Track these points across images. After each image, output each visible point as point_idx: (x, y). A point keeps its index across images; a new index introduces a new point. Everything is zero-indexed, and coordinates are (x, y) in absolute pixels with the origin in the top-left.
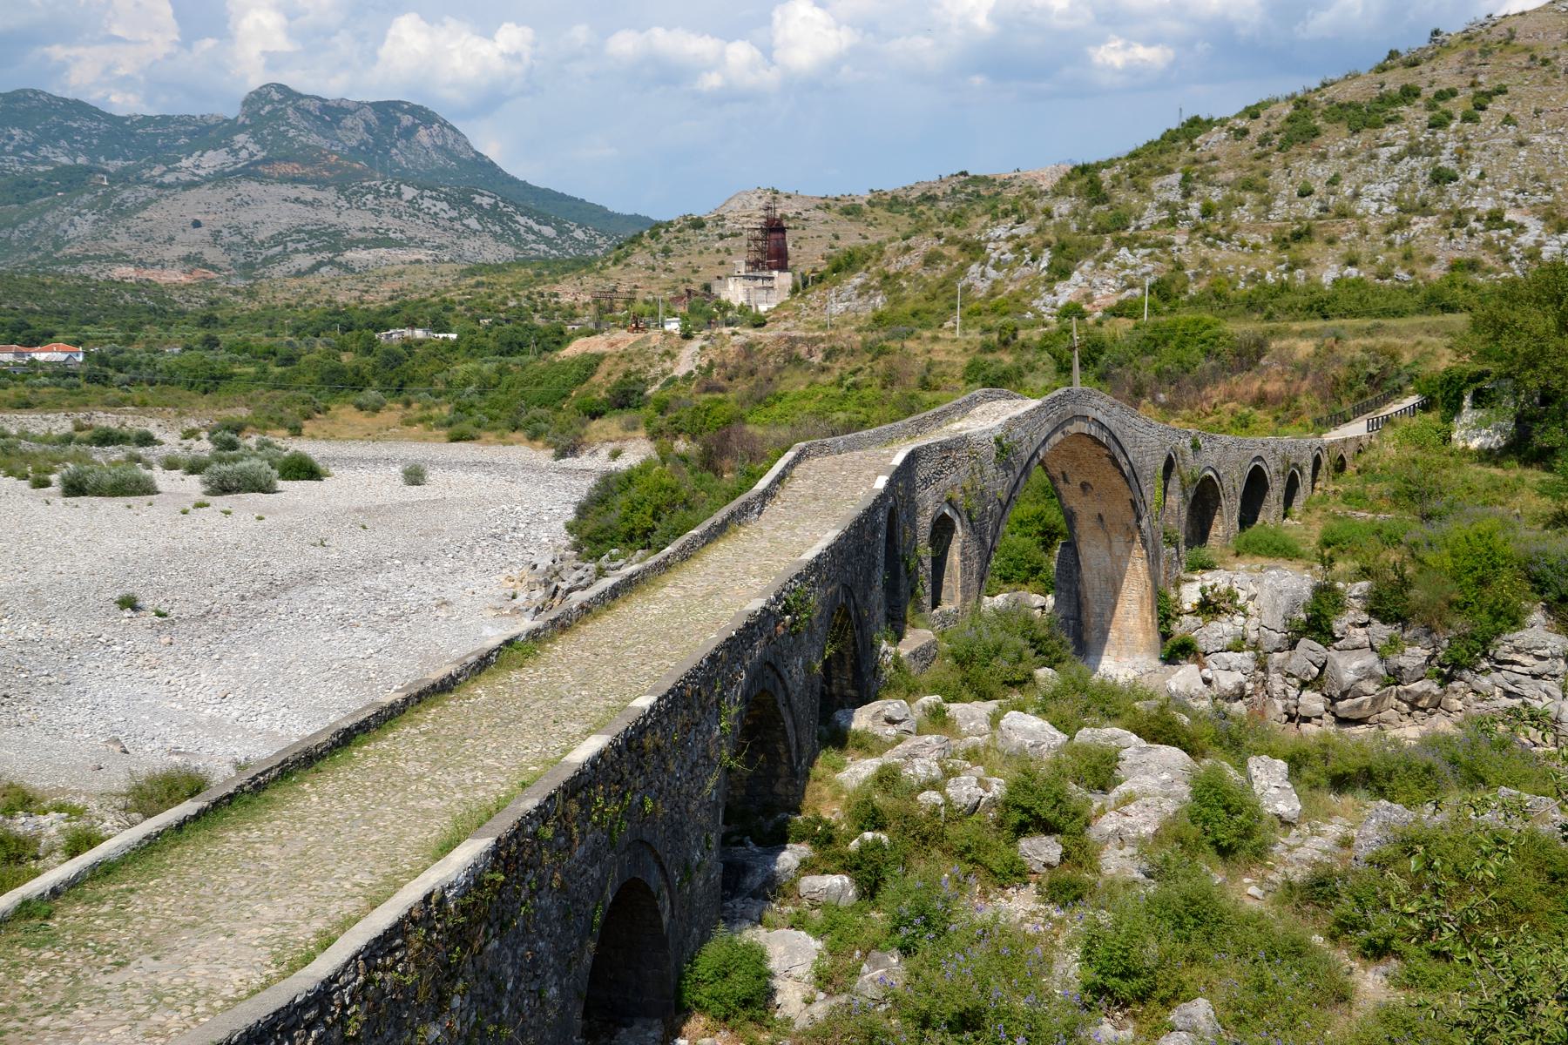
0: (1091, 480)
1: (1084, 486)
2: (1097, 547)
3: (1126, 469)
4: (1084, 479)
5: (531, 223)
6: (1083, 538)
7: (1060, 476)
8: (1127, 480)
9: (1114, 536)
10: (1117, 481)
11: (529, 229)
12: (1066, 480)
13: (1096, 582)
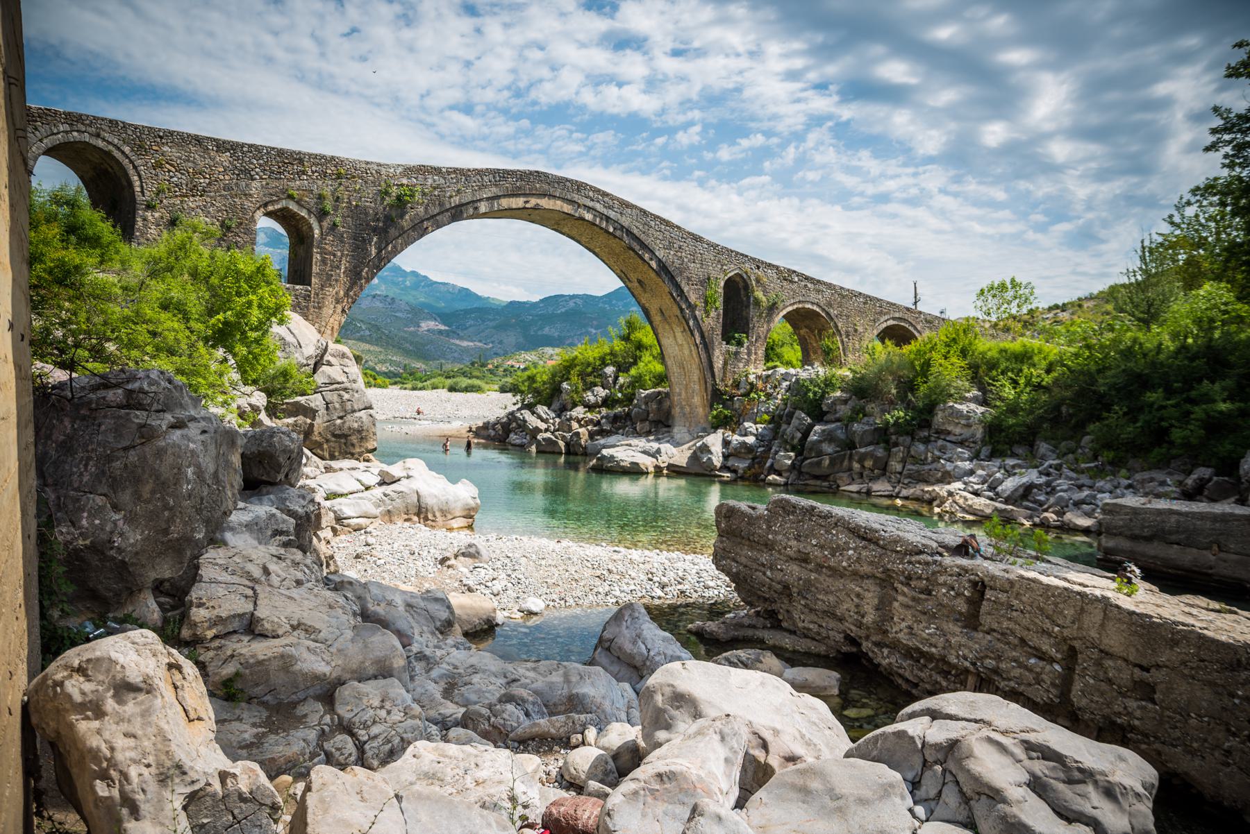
1: (640, 282)
9: (674, 326)
10: (653, 275)
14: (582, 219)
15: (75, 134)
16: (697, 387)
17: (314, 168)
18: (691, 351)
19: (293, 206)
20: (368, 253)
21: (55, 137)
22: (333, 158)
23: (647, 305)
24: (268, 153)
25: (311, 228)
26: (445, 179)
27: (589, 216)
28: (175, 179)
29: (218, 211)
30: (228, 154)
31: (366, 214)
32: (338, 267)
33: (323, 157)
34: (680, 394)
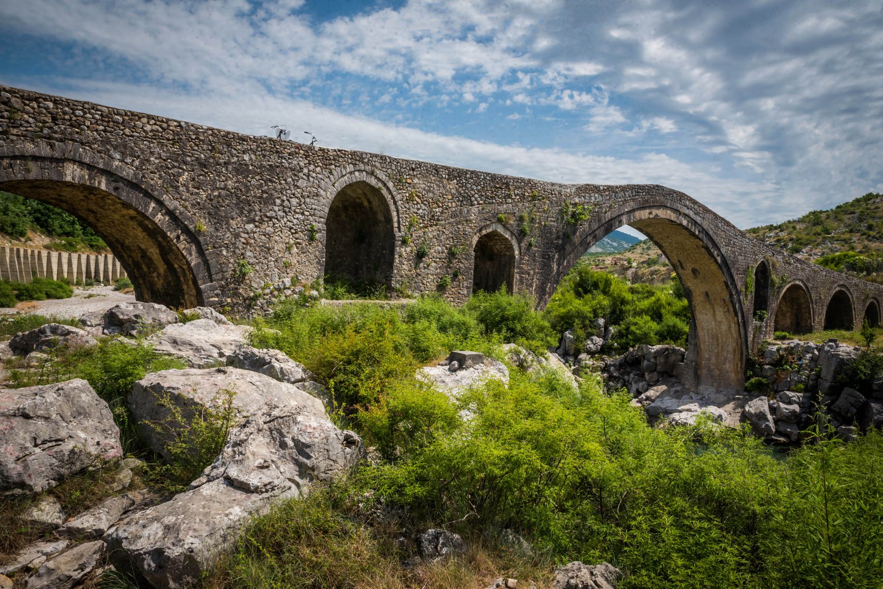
0: (697, 267)
1: (694, 271)
2: (706, 315)
3: (719, 259)
4: (693, 266)
5: (609, 241)
6: (697, 308)
7: (678, 264)
8: (720, 267)
9: (716, 307)
10: (714, 267)
11: (608, 243)
12: (683, 268)
13: (707, 340)
14: (681, 225)
15: (357, 173)
16: (730, 356)
17: (516, 192)
18: (730, 327)
19: (500, 230)
20: (551, 271)
21: (342, 179)
22: (529, 181)
23: (692, 288)
24: (485, 178)
25: (510, 248)
26: (602, 196)
27: (685, 222)
28: (421, 211)
29: (447, 239)
30: (455, 181)
31: (551, 233)
32: (532, 286)
33: (523, 180)
34: (709, 359)
